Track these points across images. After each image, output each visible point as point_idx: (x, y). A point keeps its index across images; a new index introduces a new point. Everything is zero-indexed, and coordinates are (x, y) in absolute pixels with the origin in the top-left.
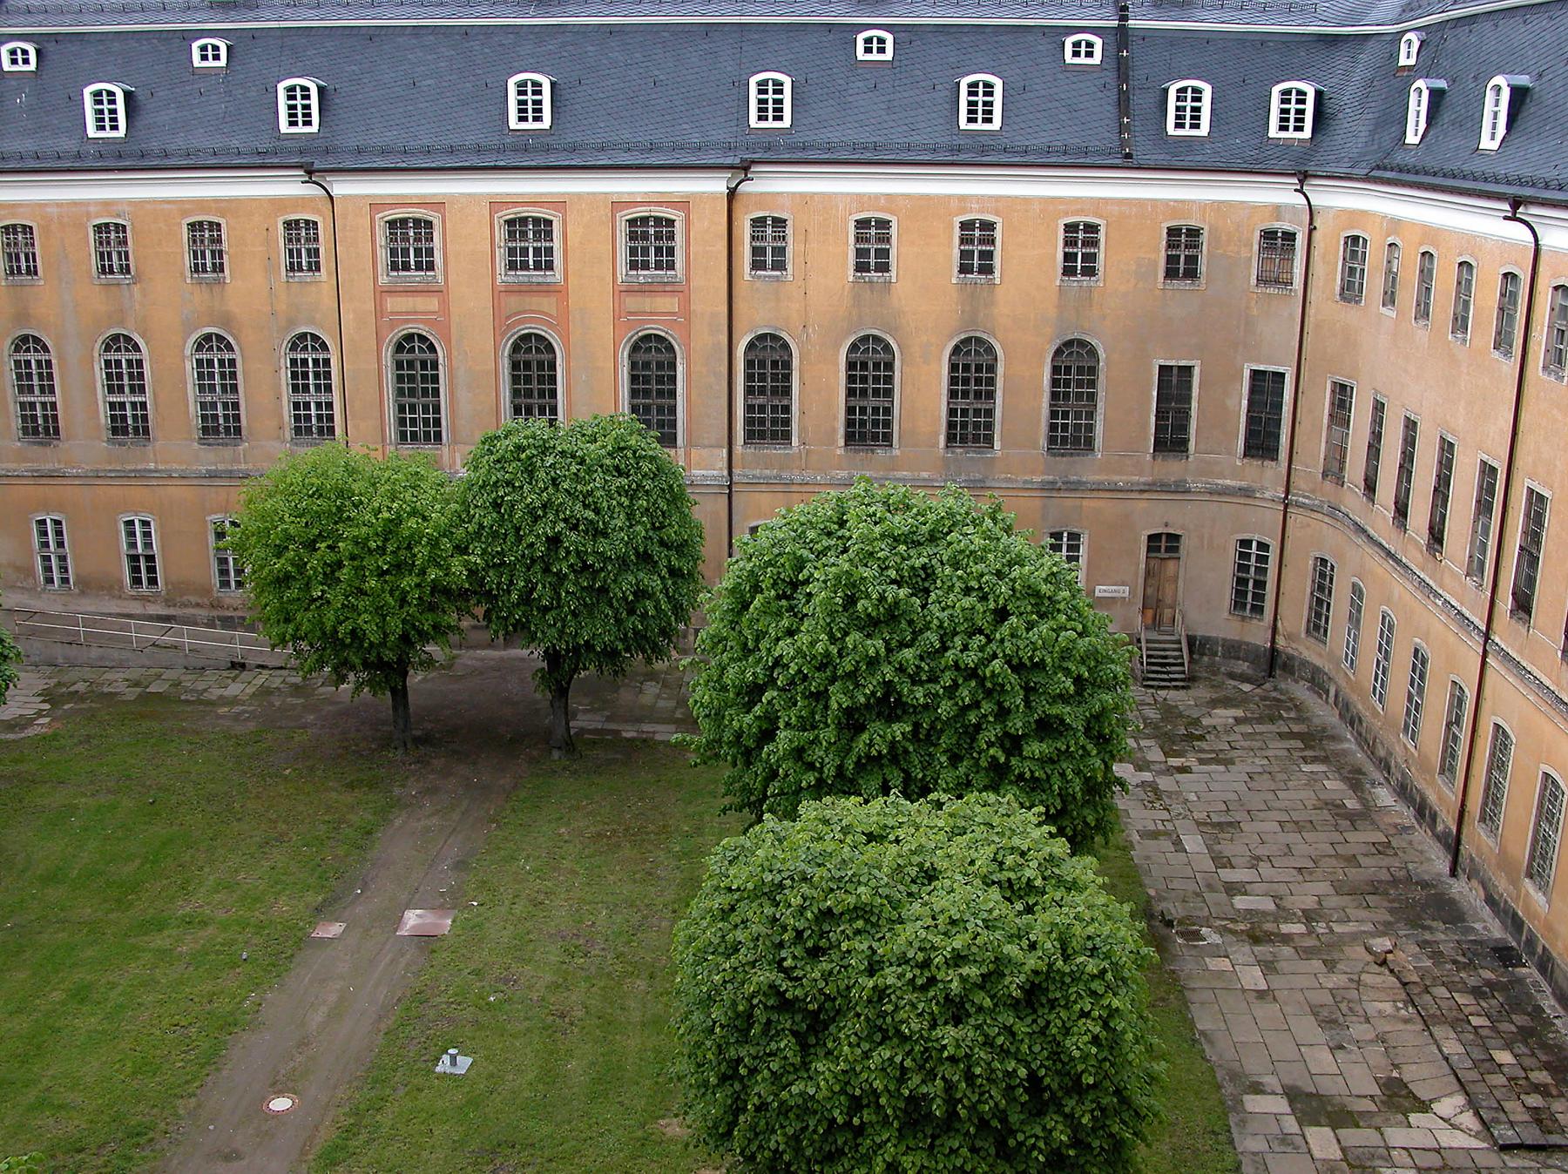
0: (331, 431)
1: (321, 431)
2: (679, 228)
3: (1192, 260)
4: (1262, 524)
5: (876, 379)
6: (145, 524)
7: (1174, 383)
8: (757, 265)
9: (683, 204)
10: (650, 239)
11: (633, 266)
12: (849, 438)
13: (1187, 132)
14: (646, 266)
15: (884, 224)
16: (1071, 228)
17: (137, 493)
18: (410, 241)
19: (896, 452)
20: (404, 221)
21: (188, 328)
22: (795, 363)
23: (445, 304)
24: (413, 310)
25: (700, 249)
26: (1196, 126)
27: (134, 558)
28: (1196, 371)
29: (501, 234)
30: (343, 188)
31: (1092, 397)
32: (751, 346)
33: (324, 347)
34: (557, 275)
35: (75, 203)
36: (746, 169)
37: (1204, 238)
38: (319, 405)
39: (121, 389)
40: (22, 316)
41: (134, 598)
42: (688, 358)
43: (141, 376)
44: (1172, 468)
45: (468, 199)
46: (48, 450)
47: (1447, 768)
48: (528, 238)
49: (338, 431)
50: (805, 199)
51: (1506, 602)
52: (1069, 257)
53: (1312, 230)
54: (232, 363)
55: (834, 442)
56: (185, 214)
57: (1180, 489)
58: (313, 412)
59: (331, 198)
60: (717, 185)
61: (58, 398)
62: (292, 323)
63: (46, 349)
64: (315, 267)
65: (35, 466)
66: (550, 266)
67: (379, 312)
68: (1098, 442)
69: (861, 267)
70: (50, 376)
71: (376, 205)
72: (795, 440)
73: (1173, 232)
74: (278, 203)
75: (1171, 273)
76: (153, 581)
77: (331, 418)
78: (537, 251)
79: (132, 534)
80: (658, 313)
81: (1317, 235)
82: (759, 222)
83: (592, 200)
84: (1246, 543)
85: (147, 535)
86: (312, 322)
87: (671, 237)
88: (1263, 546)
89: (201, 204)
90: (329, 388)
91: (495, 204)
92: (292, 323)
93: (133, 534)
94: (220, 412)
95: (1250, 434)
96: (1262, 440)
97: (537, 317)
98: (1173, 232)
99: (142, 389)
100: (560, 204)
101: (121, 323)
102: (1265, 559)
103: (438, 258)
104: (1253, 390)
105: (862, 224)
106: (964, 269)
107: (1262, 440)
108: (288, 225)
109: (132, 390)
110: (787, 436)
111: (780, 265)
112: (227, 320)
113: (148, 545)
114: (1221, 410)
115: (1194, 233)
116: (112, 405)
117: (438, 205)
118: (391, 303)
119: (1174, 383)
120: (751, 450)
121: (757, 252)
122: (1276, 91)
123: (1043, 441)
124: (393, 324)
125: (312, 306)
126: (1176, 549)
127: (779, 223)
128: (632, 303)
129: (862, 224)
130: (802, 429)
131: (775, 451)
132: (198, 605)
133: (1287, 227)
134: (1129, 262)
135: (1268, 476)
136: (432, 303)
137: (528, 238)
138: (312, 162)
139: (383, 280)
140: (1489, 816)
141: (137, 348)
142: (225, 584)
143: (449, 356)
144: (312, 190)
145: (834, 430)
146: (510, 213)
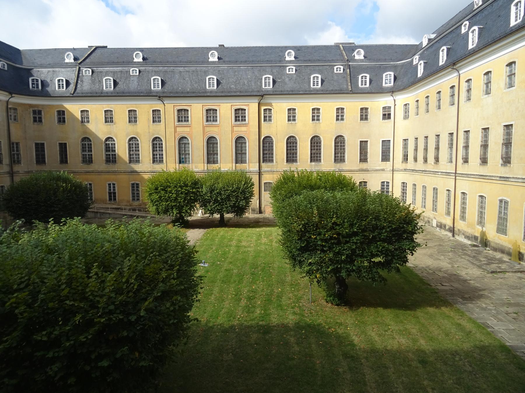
0: (163, 161)
1: (160, 161)
3: (366, 116)
4: (386, 177)
5: (293, 146)
6: (114, 184)
7: (363, 145)
8: (265, 120)
10: (240, 115)
12: (287, 161)
13: (364, 86)
14: (239, 120)
15: (294, 109)
17: (113, 177)
19: (298, 163)
21: (127, 135)
22: (274, 143)
24: (183, 131)
26: (365, 85)
27: (110, 193)
28: (369, 142)
31: (344, 149)
32: (264, 139)
33: (161, 140)
34: (218, 122)
36: (262, 96)
38: (160, 155)
41: (110, 204)
44: (364, 166)
46: (89, 166)
47: (448, 213)
49: (164, 161)
51: (460, 161)
52: (337, 116)
54: (138, 144)
56: (127, 108)
57: (367, 170)
58: (158, 156)
61: (93, 153)
62: (153, 134)
63: (90, 141)
68: (346, 160)
69: (289, 120)
70: (91, 148)
75: (361, 119)
76: (115, 199)
77: (162, 158)
79: (110, 187)
80: (241, 131)
84: (383, 182)
85: (114, 187)
86: (158, 134)
87: (245, 113)
88: (388, 183)
90: (162, 150)
92: (153, 134)
94: (134, 156)
96: (385, 157)
97: (212, 131)
101: (110, 134)
102: (388, 186)
103: (189, 119)
107: (385, 157)
108: (153, 111)
110: (272, 161)
112: (137, 134)
113: (114, 190)
114: (375, 151)
116: (107, 155)
119: (363, 145)
121: (265, 117)
122: (384, 75)
123: (333, 160)
125: (159, 130)
126: (366, 185)
131: (270, 164)
132: (126, 205)
135: (388, 165)
136: (187, 129)
139: (176, 123)
140: (463, 218)
142: (133, 200)
145: (284, 159)
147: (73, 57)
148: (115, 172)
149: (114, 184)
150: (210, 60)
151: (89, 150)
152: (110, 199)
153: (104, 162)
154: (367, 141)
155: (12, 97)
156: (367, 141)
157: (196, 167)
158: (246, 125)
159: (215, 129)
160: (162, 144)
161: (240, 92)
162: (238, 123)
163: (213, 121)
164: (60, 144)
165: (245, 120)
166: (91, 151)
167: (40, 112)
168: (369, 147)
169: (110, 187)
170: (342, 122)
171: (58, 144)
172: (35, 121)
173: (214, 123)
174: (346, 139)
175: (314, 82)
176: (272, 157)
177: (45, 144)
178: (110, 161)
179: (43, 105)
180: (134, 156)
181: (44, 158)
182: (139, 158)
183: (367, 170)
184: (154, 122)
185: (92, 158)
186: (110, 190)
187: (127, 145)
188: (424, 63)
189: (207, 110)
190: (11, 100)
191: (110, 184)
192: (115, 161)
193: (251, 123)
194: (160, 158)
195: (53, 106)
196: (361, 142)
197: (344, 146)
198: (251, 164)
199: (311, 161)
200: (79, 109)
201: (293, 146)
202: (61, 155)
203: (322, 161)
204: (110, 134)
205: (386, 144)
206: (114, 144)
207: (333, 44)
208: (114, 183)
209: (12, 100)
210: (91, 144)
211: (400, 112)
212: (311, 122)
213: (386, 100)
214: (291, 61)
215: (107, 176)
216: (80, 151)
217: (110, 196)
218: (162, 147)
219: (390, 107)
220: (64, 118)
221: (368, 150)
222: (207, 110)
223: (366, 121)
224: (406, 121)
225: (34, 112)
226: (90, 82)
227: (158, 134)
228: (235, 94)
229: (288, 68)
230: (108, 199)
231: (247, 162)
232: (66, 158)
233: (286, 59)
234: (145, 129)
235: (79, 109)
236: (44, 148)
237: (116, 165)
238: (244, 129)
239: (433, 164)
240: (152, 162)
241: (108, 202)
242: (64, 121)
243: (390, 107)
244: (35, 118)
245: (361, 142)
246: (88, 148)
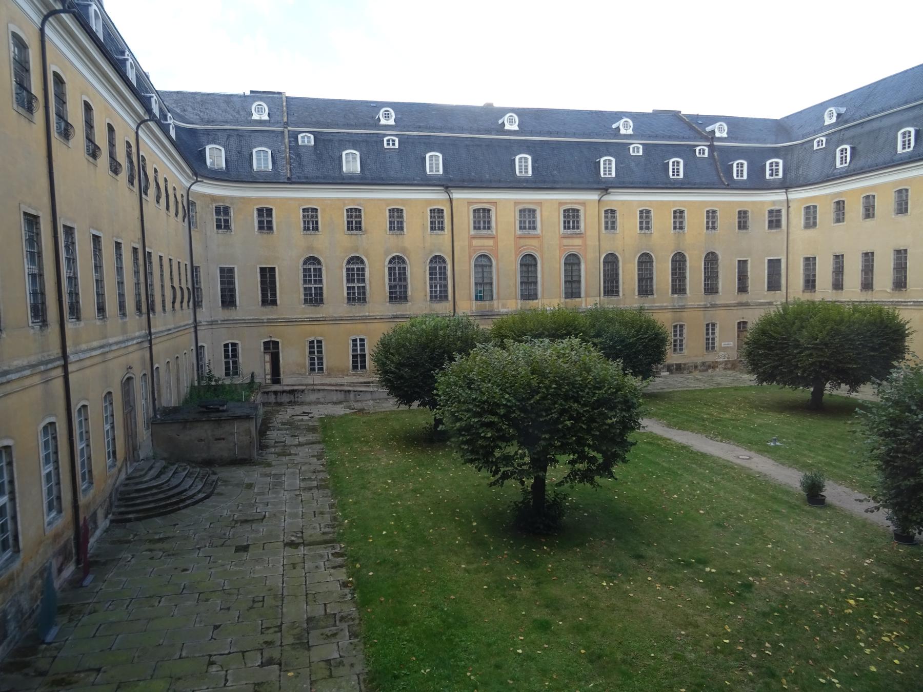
0: (446, 297)
1: (441, 297)
2: (582, 213)
6: (362, 340)
8: (606, 228)
9: (583, 203)
10: (571, 218)
11: (565, 228)
16: (708, 212)
17: (360, 327)
18: (482, 218)
20: (479, 210)
21: (386, 253)
22: (620, 264)
23: (496, 243)
25: (590, 221)
27: (355, 357)
28: (749, 262)
29: (517, 214)
30: (457, 195)
33: (444, 261)
34: (539, 231)
35: (339, 199)
37: (750, 214)
38: (441, 286)
39: (353, 281)
40: (310, 248)
41: (354, 375)
42: (586, 263)
43: (363, 275)
44: (744, 298)
45: (505, 202)
48: (528, 217)
50: (623, 202)
53: (788, 207)
55: (634, 294)
56: (388, 205)
59: (451, 200)
60: (593, 196)
62: (431, 251)
63: (319, 263)
64: (442, 229)
65: (311, 316)
66: (534, 228)
67: (470, 246)
68: (720, 289)
69: (641, 228)
70: (320, 276)
71: (470, 202)
72: (621, 294)
73: (740, 212)
74: (429, 202)
75: (740, 228)
77: (446, 291)
78: (530, 222)
81: (791, 209)
82: (606, 211)
83: (551, 203)
85: (362, 345)
86: (440, 250)
87: (578, 216)
89: (395, 201)
90: (445, 279)
91: (517, 203)
92: (431, 251)
93: (356, 345)
94: (398, 289)
95: (769, 283)
97: (531, 246)
98: (740, 212)
99: (364, 281)
100: (540, 203)
101: (357, 251)
103: (493, 224)
104: (769, 267)
105: (641, 212)
106: (675, 228)
108: (432, 211)
109: (358, 281)
110: (617, 293)
111: (613, 228)
112: (404, 250)
113: (363, 350)
115: (745, 212)
117: (494, 203)
118: (476, 242)
120: (606, 298)
121: (606, 223)
122: (768, 163)
123: (703, 290)
124: (475, 251)
127: (613, 212)
128: (566, 242)
129: (641, 212)
130: (623, 290)
133: (777, 208)
134: (727, 222)
136: (490, 242)
137: (528, 217)
138: (446, 184)
141: (362, 262)
143: (498, 264)
144: (443, 196)
145: (634, 289)
146: (521, 207)
147: (267, 111)
148: (363, 319)
149: (362, 340)
150: (506, 128)
151: (315, 281)
152: (355, 367)
153: (346, 301)
154: (746, 261)
155: (197, 181)
156: (746, 261)
157: (504, 306)
158: (580, 236)
159: (534, 242)
160: (445, 268)
161: (572, 182)
162: (569, 232)
163: (530, 228)
164: (263, 270)
165: (578, 228)
166: (321, 281)
167: (226, 210)
168: (749, 269)
169: (355, 345)
170: (714, 231)
171: (258, 270)
172: (219, 227)
173: (531, 232)
174: (720, 257)
175: (605, 168)
176: (617, 287)
177: (236, 270)
178: (354, 299)
179: (232, 198)
180: (398, 289)
181: (233, 296)
182: (406, 292)
183: (714, 306)
184: (432, 229)
185: (321, 294)
186: (355, 350)
187: (387, 270)
188: (852, 148)
189: (520, 211)
190: (194, 188)
191: (355, 341)
192: (364, 299)
193: (588, 233)
194: (441, 291)
195: (250, 199)
196: (739, 261)
197: (717, 268)
198: (588, 299)
199: (673, 293)
200: (300, 206)
201: (646, 270)
202: (264, 290)
203: (688, 292)
204: (357, 251)
205: (774, 265)
206: (363, 269)
207: (649, 110)
208: (363, 337)
209: (197, 188)
210: (320, 270)
211: (798, 219)
212: (672, 231)
213: (776, 197)
214: (631, 135)
215: (349, 326)
216: (301, 282)
217: (355, 362)
218: (445, 273)
219: (779, 211)
220: (270, 222)
221: (749, 274)
222: (520, 211)
223: (744, 231)
224: (810, 232)
225: (218, 210)
226: (313, 157)
227: (440, 250)
228: (563, 185)
229: (631, 147)
230: (351, 367)
231: (583, 294)
232: (274, 294)
233: (506, 128)
234: (417, 241)
235: (300, 206)
236: (232, 277)
237: (367, 305)
238: (577, 242)
239: (889, 290)
240: (428, 298)
241: (351, 372)
242: (270, 228)
243: (779, 211)
244: (218, 220)
245: (739, 261)
246: (440, 274)
